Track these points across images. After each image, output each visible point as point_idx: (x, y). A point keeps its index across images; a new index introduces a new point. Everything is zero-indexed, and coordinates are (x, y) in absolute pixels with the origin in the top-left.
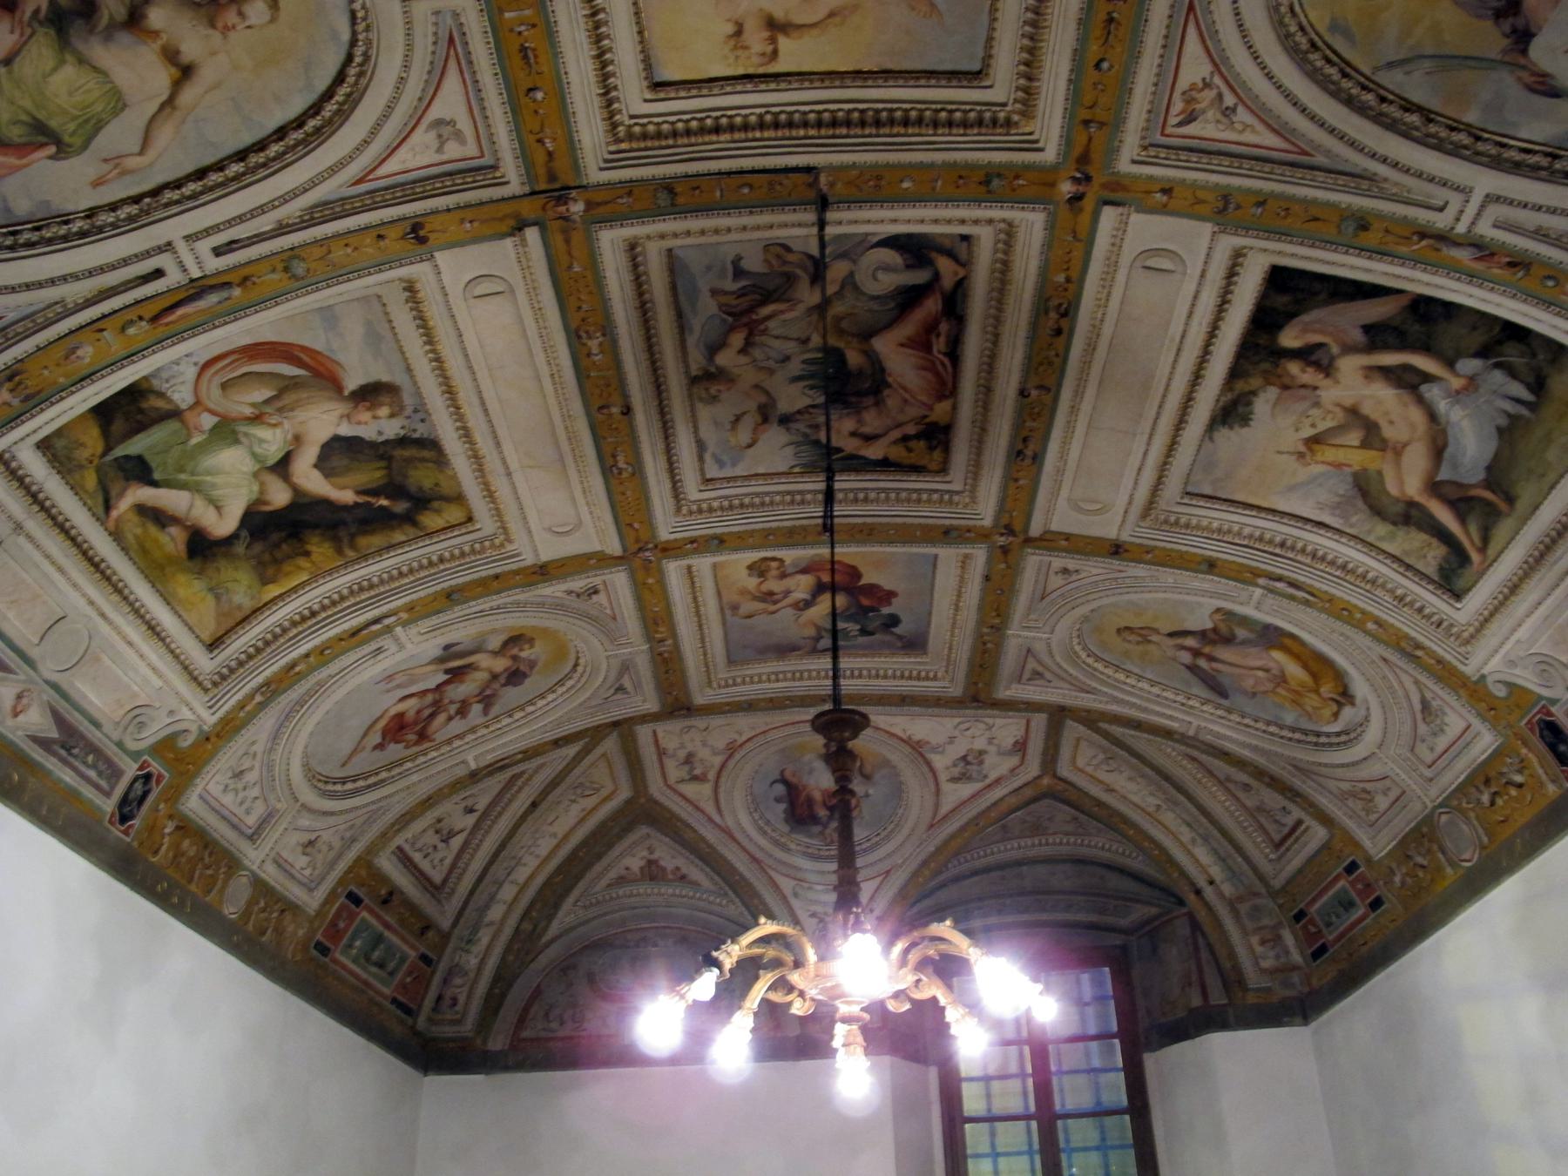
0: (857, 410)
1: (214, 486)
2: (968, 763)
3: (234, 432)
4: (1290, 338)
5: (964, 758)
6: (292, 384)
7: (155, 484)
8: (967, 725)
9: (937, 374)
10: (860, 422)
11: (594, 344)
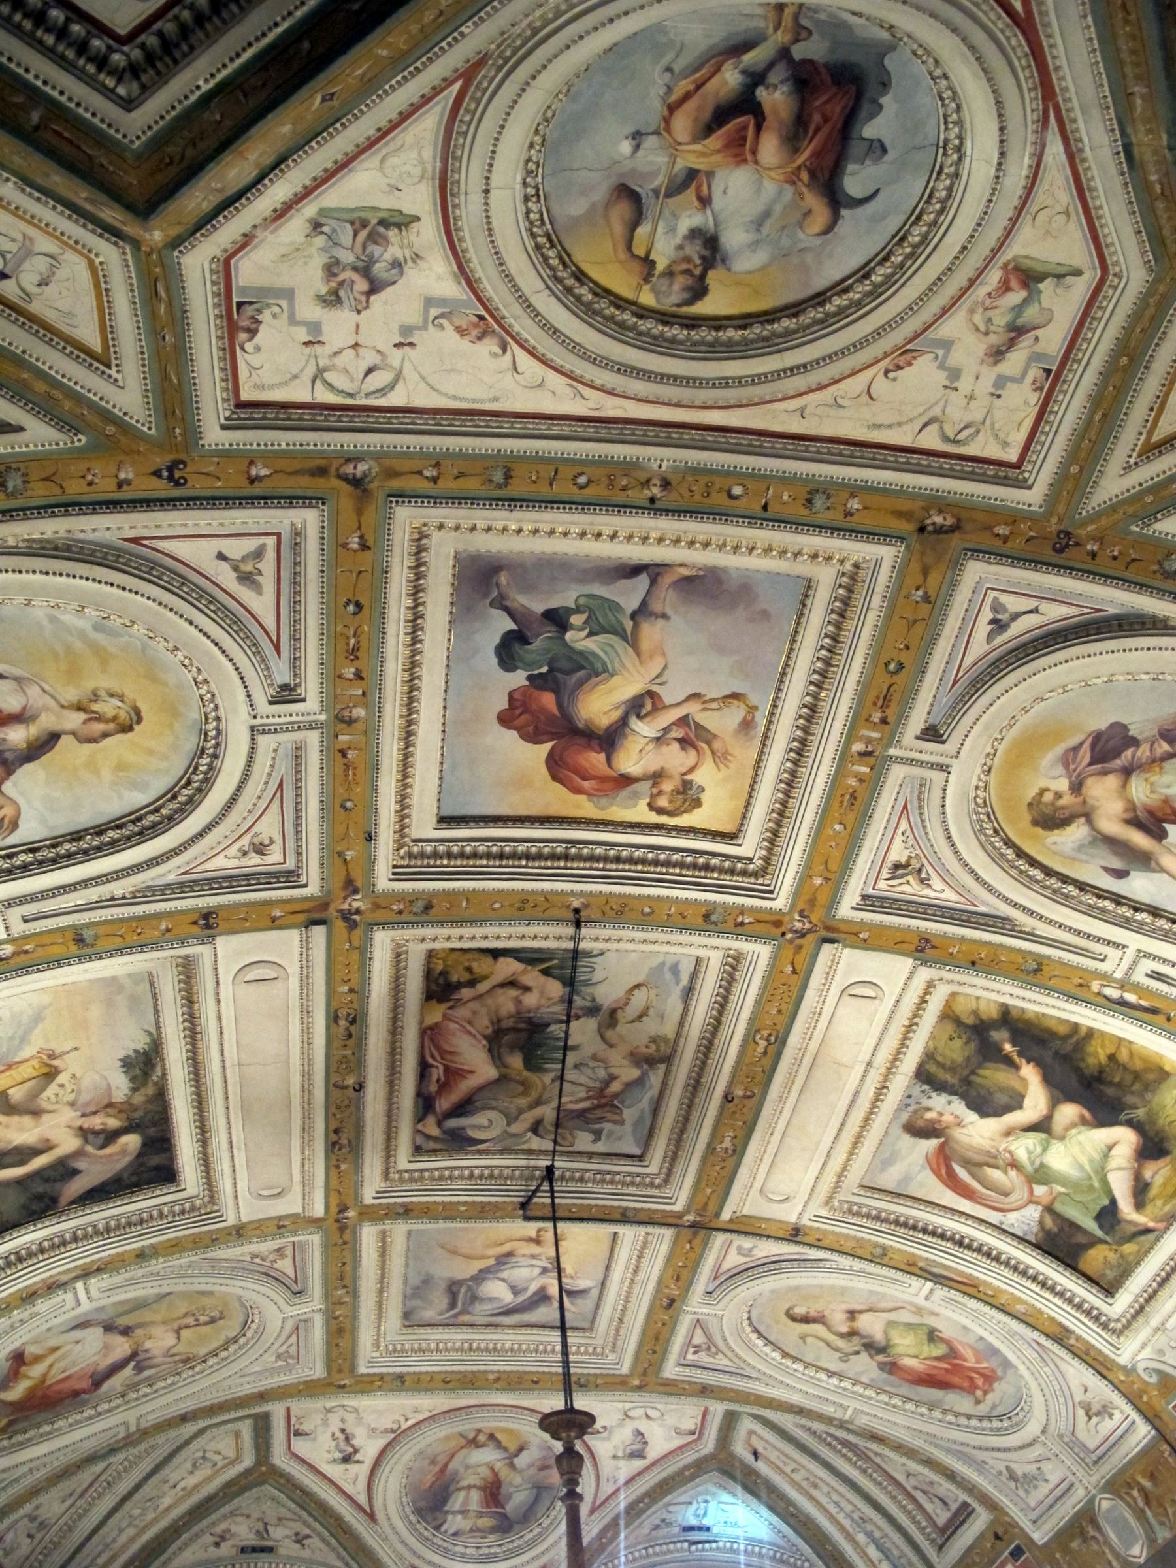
0: (518, 1015)
1: (1091, 1161)
2: (365, 270)
3: (1036, 1171)
4: (132, 1141)
5: (375, 287)
6: (967, 1163)
7: (1113, 1202)
8: (379, 379)
9: (438, 1048)
10: (518, 1002)
11: (727, 1143)
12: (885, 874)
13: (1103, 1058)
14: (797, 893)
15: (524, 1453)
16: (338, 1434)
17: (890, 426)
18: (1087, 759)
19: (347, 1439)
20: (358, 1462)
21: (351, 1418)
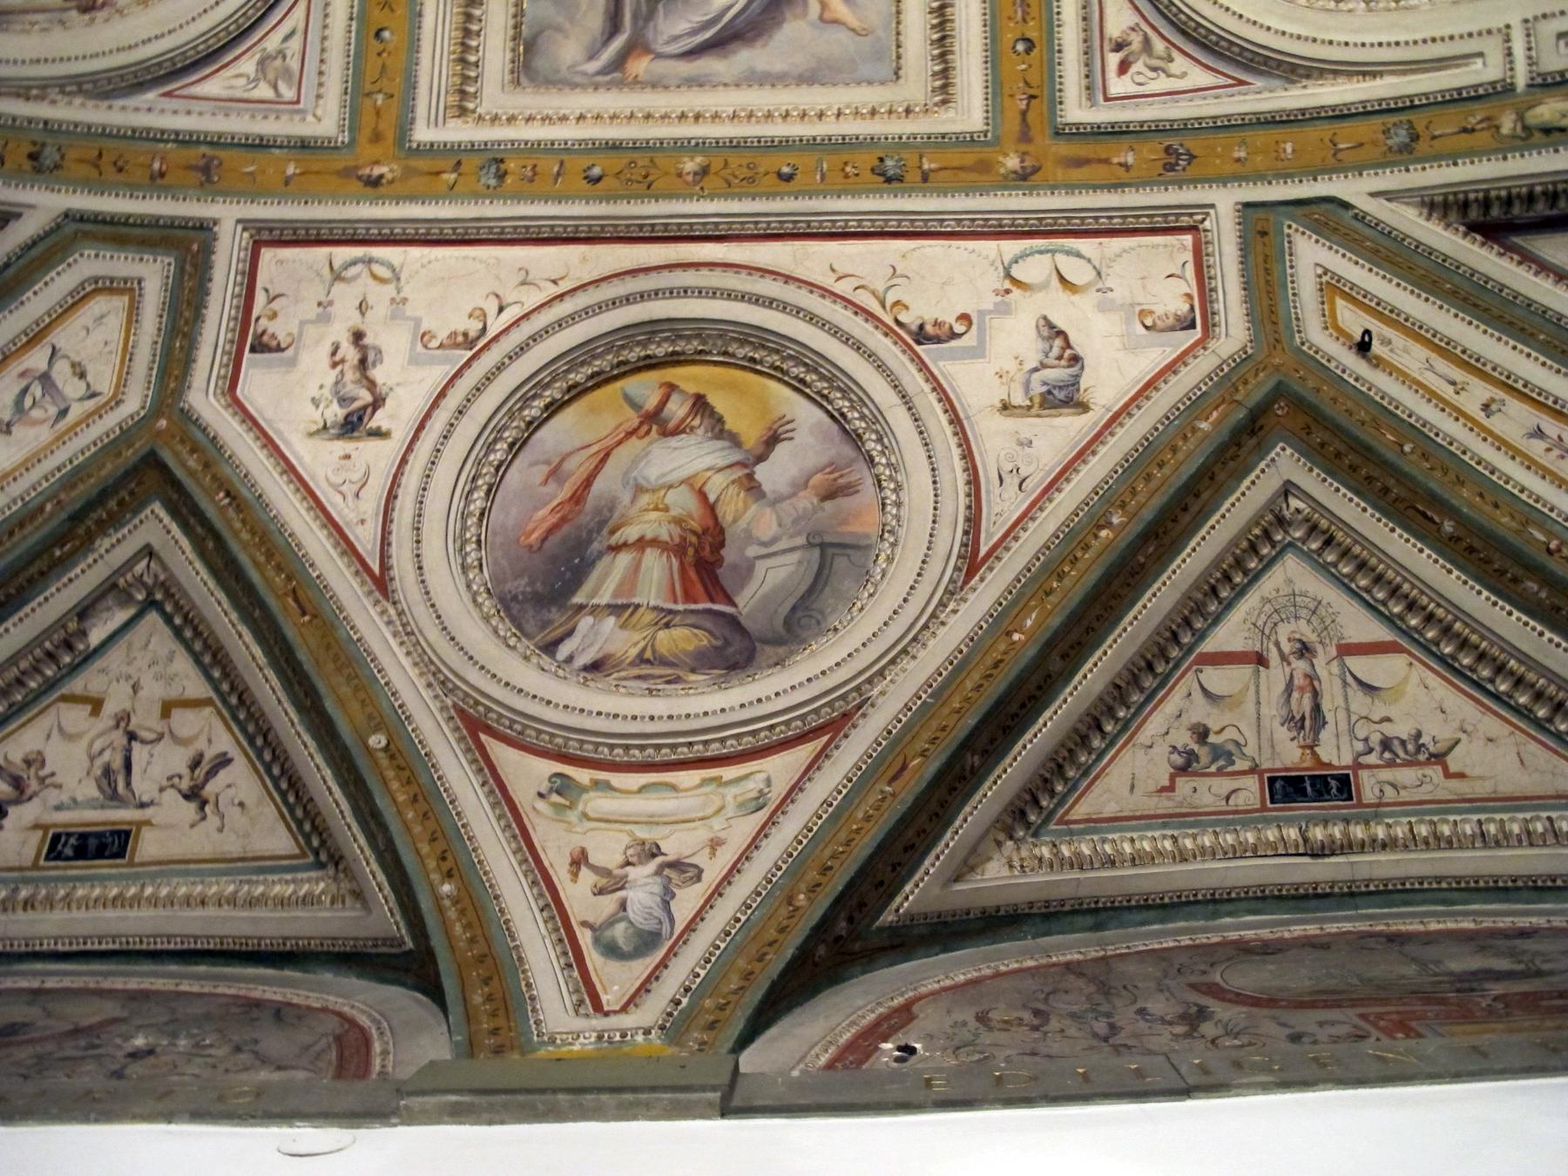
15: (781, 450)
16: (350, 354)
19: (363, 363)
20: (378, 434)
21: (380, 296)
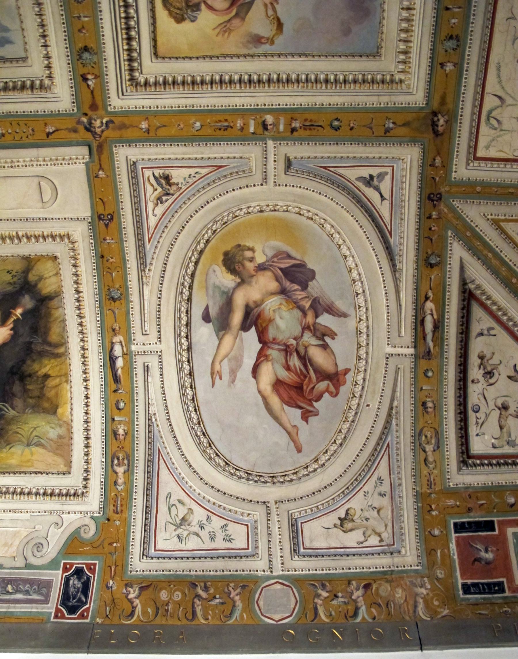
12: (157, 173)
13: (44, 371)
14: (128, 113)
17: (499, 76)
18: (283, 266)
